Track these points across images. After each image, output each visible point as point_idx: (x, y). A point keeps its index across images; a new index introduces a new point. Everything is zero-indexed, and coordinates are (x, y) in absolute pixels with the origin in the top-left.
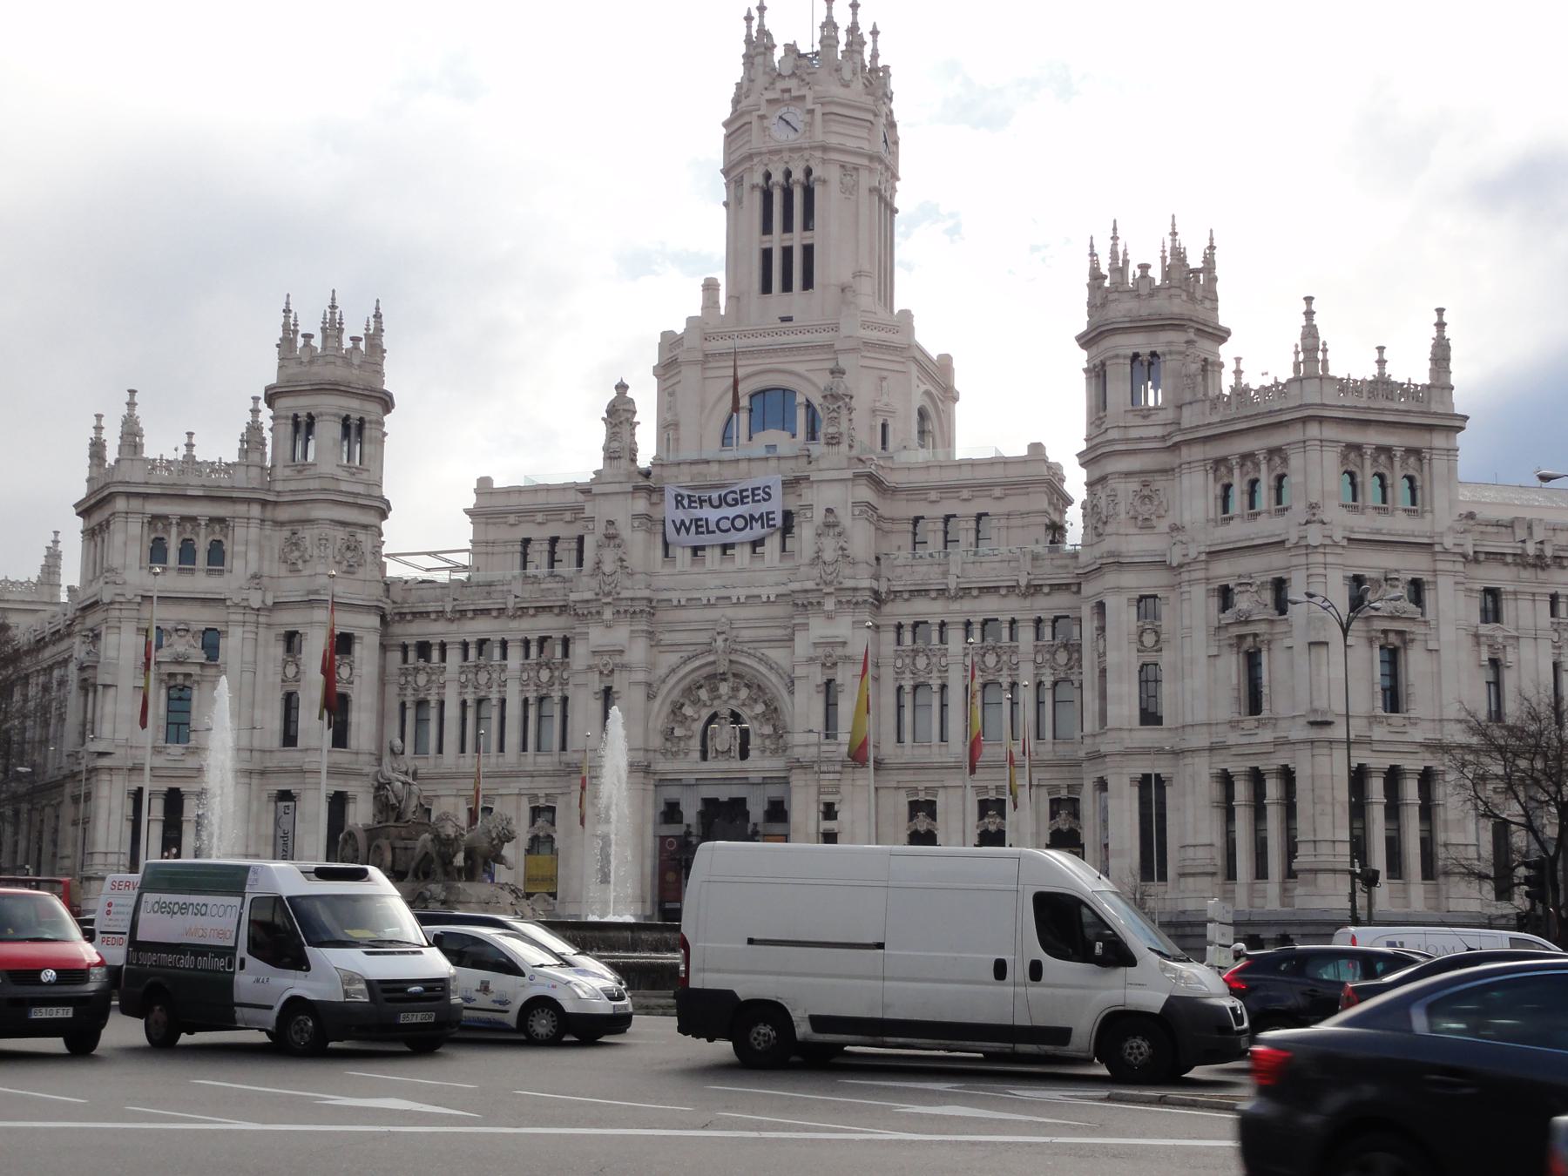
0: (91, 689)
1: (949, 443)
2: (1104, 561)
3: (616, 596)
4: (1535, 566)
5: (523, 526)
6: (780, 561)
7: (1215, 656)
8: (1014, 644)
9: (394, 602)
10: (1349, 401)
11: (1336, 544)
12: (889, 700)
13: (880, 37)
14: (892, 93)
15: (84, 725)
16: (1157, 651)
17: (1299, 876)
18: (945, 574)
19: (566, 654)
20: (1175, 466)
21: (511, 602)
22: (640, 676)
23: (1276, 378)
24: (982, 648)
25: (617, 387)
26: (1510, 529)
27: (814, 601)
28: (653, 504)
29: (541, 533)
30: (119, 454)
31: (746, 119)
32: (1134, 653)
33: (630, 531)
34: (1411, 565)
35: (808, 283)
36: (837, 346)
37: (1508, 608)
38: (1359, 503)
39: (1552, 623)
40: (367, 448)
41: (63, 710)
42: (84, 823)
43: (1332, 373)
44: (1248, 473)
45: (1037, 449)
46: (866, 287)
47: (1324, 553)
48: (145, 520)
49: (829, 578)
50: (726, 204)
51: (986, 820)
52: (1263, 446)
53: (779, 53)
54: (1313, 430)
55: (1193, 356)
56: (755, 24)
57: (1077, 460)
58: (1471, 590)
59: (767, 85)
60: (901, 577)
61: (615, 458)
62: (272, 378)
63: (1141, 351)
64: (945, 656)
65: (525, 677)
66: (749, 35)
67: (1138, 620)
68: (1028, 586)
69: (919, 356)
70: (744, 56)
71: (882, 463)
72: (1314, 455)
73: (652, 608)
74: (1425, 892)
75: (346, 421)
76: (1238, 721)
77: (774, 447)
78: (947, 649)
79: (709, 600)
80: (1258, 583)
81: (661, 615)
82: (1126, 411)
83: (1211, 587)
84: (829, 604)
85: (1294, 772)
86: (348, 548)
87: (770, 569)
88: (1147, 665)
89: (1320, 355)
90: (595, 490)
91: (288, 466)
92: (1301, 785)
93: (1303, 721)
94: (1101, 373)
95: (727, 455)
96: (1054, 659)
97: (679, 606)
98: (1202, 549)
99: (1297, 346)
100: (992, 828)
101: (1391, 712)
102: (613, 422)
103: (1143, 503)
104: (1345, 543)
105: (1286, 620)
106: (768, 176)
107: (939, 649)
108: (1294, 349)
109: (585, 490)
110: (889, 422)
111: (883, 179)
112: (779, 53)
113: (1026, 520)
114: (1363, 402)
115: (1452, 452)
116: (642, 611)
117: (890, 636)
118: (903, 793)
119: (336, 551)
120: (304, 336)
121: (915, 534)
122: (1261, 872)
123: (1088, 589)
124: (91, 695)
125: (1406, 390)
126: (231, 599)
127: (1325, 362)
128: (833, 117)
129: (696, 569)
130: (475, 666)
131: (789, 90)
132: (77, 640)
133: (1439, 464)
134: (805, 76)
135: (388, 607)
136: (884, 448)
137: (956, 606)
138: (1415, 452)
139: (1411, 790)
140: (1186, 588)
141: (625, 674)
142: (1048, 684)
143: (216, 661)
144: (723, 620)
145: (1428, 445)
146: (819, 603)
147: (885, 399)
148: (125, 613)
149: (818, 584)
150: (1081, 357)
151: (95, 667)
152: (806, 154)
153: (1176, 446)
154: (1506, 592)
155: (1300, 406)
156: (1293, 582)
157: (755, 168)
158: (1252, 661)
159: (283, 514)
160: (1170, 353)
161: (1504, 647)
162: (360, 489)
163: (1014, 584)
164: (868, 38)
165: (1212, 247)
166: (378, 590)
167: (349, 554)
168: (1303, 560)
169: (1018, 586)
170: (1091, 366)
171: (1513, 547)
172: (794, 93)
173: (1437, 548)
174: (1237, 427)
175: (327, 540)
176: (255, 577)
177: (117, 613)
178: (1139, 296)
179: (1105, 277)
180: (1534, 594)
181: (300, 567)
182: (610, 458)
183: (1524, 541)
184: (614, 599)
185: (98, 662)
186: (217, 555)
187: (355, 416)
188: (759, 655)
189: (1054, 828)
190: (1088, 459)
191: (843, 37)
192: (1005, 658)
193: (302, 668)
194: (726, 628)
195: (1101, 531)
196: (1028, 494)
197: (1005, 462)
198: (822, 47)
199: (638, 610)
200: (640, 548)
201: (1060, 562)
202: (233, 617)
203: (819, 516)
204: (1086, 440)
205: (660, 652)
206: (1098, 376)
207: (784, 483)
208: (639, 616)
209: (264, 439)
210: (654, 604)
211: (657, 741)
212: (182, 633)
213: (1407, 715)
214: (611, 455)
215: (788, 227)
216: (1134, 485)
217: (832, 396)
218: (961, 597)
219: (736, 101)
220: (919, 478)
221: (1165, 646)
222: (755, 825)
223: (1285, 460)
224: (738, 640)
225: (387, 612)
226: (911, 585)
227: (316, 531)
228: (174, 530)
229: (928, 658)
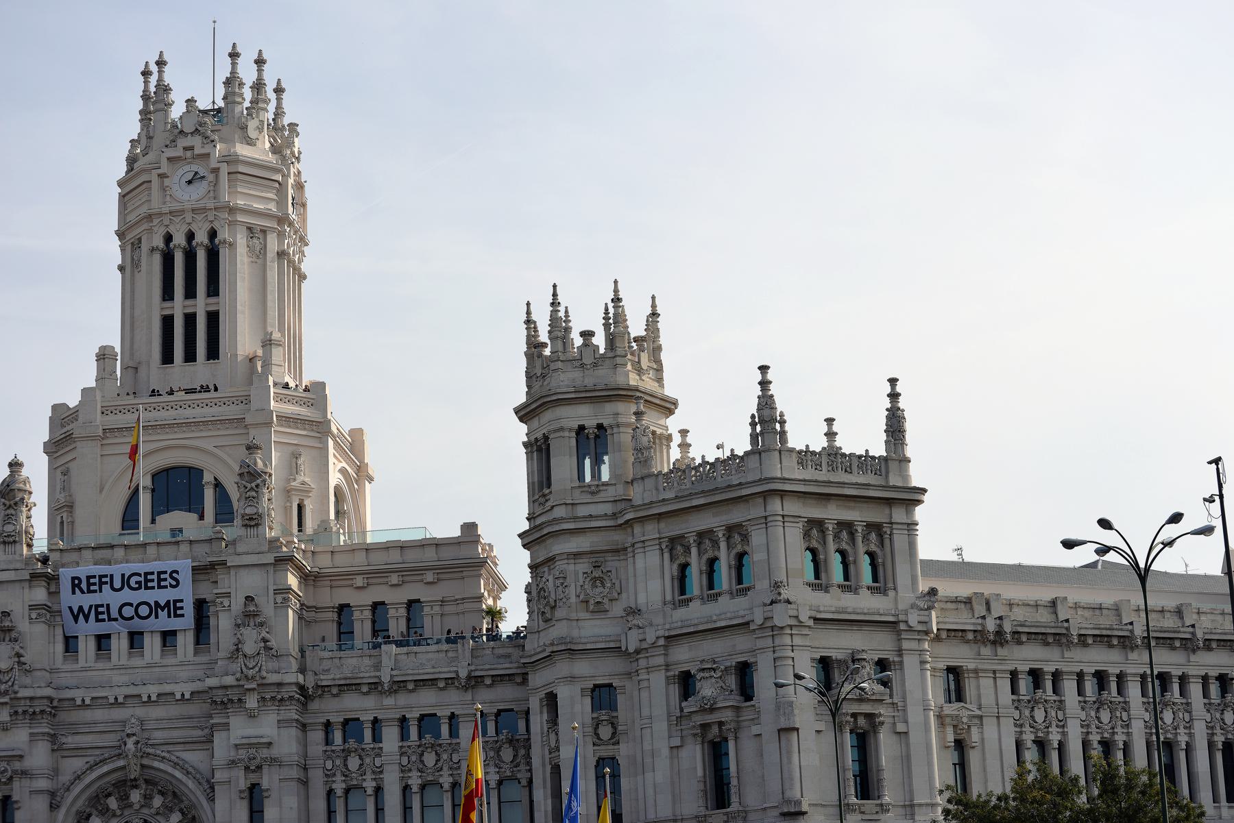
2: (555, 649)
3: (13, 696)
4: (994, 643)
6: (196, 653)
7: (678, 747)
8: (454, 741)
10: (809, 474)
11: (801, 625)
18: (377, 667)
20: (626, 545)
22: (43, 784)
23: (732, 450)
25: (10, 465)
26: (968, 606)
27: (235, 698)
32: (591, 748)
33: (28, 621)
34: (874, 645)
35: (213, 352)
36: (249, 420)
38: (823, 581)
39: (1013, 701)
43: (790, 444)
44: (706, 551)
45: (470, 529)
47: (791, 635)
49: (251, 673)
50: (121, 268)
52: (725, 523)
54: (776, 506)
56: (153, 80)
57: (519, 541)
59: (168, 143)
60: (328, 670)
61: (9, 543)
66: (146, 90)
67: (592, 712)
68: (469, 677)
70: (141, 112)
71: (303, 547)
73: (52, 708)
76: (705, 816)
77: (181, 531)
78: (382, 748)
79: (116, 699)
80: (722, 667)
81: (63, 716)
83: (671, 673)
84: (252, 702)
87: (182, 664)
88: (603, 759)
89: (778, 426)
93: (776, 813)
94: (544, 447)
95: (127, 540)
96: (499, 756)
97: (83, 706)
98: (661, 633)
99: (753, 416)
101: (862, 799)
102: (8, 503)
103: (594, 586)
104: (811, 623)
105: (754, 706)
106: (168, 238)
107: (373, 749)
110: (306, 503)
112: (177, 111)
113: (461, 607)
114: (823, 475)
116: (42, 712)
117: (317, 736)
121: (340, 624)
123: (538, 679)
125: (865, 461)
127: (783, 433)
128: (240, 176)
129: (100, 665)
131: (191, 148)
133: (899, 539)
136: (299, 531)
137: (389, 701)
141: (26, 782)
144: (133, 721)
146: (240, 700)
147: (300, 478)
149: (238, 680)
150: (521, 431)
155: (760, 480)
157: (155, 229)
158: (717, 753)
163: (453, 675)
165: (654, 314)
168: (769, 642)
170: (532, 439)
171: (974, 624)
172: (197, 151)
173: (902, 626)
174: (695, 502)
178: (582, 365)
179: (544, 345)
180: (994, 672)
183: (984, 617)
188: (173, 758)
190: (529, 540)
191: (248, 94)
192: (445, 756)
194: (136, 730)
195: (548, 616)
197: (437, 544)
198: (226, 104)
199: (38, 710)
201: (501, 651)
203: (237, 604)
204: (528, 519)
205: (63, 757)
206: (539, 450)
207: (194, 569)
208: (40, 717)
210: (55, 703)
213: (879, 802)
215: (190, 293)
216: (583, 566)
218: (396, 691)
219: (131, 160)
220: (343, 563)
221: (622, 738)
223: (745, 538)
224: (150, 742)
226: (340, 679)
229: (361, 758)
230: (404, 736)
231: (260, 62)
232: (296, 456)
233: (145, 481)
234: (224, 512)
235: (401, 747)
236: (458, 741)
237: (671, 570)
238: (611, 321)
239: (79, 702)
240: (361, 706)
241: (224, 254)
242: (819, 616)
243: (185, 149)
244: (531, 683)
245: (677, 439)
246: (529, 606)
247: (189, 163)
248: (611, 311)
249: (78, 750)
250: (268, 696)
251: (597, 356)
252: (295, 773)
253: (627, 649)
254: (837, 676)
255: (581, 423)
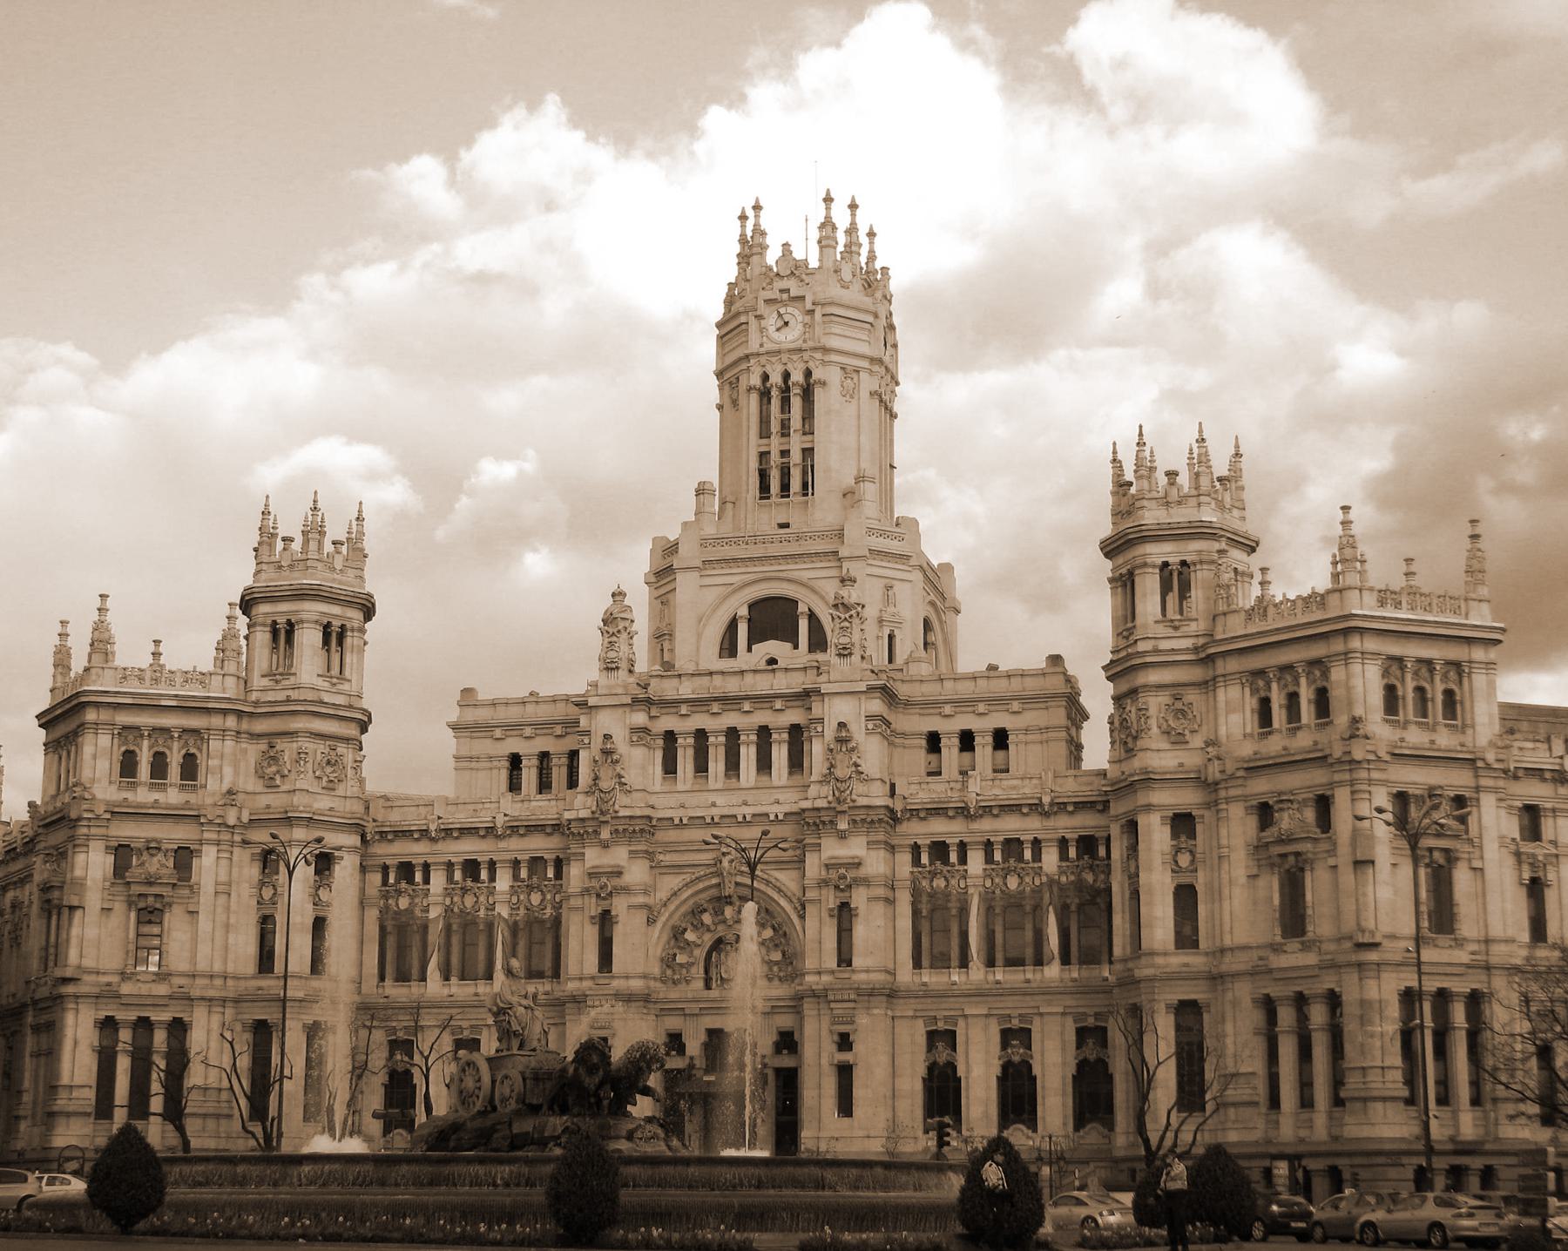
0: (55, 912)
1: (951, 659)
2: (1136, 778)
5: (509, 740)
9: (374, 821)
11: (1379, 759)
12: (905, 923)
13: (877, 240)
14: (891, 296)
15: (46, 949)
16: (1192, 872)
17: (1347, 1104)
19: (559, 875)
21: (500, 821)
22: (641, 899)
24: (1003, 869)
25: (614, 595)
27: (826, 819)
28: (651, 718)
29: (529, 749)
30: (89, 661)
31: (743, 319)
34: (1455, 780)
36: (843, 552)
37: (1548, 827)
40: (348, 659)
41: (18, 933)
42: (50, 1055)
46: (870, 490)
48: (116, 732)
50: (720, 407)
51: (1009, 1051)
53: (772, 256)
54: (1355, 643)
55: (1225, 565)
56: (750, 225)
58: (1511, 807)
59: (764, 285)
61: (612, 669)
62: (249, 582)
63: (1171, 560)
64: (965, 878)
65: (514, 900)
68: (1052, 804)
69: (925, 565)
72: (1356, 668)
74: (1474, 1119)
75: (326, 629)
76: (1281, 944)
81: (661, 836)
82: (1156, 622)
83: (1249, 804)
85: (1340, 996)
86: (329, 762)
90: (592, 701)
91: (321, 676)
92: (1350, 1008)
99: (1334, 556)
100: (1016, 1059)
102: (611, 631)
104: (1387, 758)
105: (1330, 838)
106: (765, 377)
108: (1331, 559)
109: (582, 704)
110: (895, 633)
111: (883, 383)
112: (772, 256)
115: (1492, 666)
116: (642, 831)
117: (905, 858)
118: (920, 1023)
119: (316, 766)
120: (284, 539)
122: (1306, 1102)
123: (1117, 808)
124: (54, 918)
126: (205, 816)
128: (833, 318)
130: (462, 889)
131: (788, 291)
132: (38, 861)
133: (1479, 680)
134: (804, 276)
135: (370, 828)
136: (890, 661)
138: (1457, 665)
139: (1459, 1015)
140: (1224, 806)
142: (1073, 908)
143: (189, 881)
145: (1466, 659)
148: (94, 831)
151: (61, 888)
152: (806, 356)
153: (1209, 660)
154: (1545, 809)
156: (1337, 799)
159: (261, 726)
160: (1201, 562)
161: (1545, 865)
162: (340, 700)
163: (1037, 802)
164: (864, 240)
165: (1238, 455)
166: (358, 808)
167: (329, 769)
168: (1347, 776)
169: (1041, 804)
170: (1117, 574)
173: (1480, 764)
175: (307, 753)
176: (230, 792)
177: (84, 831)
179: (1131, 484)
181: (278, 782)
182: (607, 669)
183: (1561, 757)
184: (612, 818)
185: (64, 882)
186: (190, 769)
187: (336, 623)
188: (766, 877)
189: (1080, 1058)
191: (842, 239)
193: (279, 889)
195: (1130, 745)
196: (1047, 708)
200: (642, 765)
202: (206, 835)
203: (830, 732)
206: (1125, 586)
209: (240, 647)
210: (654, 823)
211: (656, 970)
212: (154, 852)
214: (610, 667)
217: (840, 605)
219: (729, 301)
220: (930, 690)
222: (764, 1057)
223: (1325, 674)
225: (368, 830)
227: (295, 745)
228: (146, 743)
229: (946, 879)
230: (989, 859)
231: (853, 206)
232: (889, 588)
233: (744, 611)
234: (818, 641)
235: (985, 869)
236: (1040, 865)
237: (1251, 703)
238: (1195, 461)
239: (677, 821)
240: (947, 829)
241: (819, 394)
242: (1397, 752)
243: (782, 291)
244: (1112, 812)
245: (1258, 577)
246: (1111, 736)
247: (786, 305)
248: (1196, 451)
249: (677, 868)
250: (858, 818)
251: (1181, 494)
252: (881, 892)
253: (1206, 779)
254: (1414, 813)
255: (1164, 559)
